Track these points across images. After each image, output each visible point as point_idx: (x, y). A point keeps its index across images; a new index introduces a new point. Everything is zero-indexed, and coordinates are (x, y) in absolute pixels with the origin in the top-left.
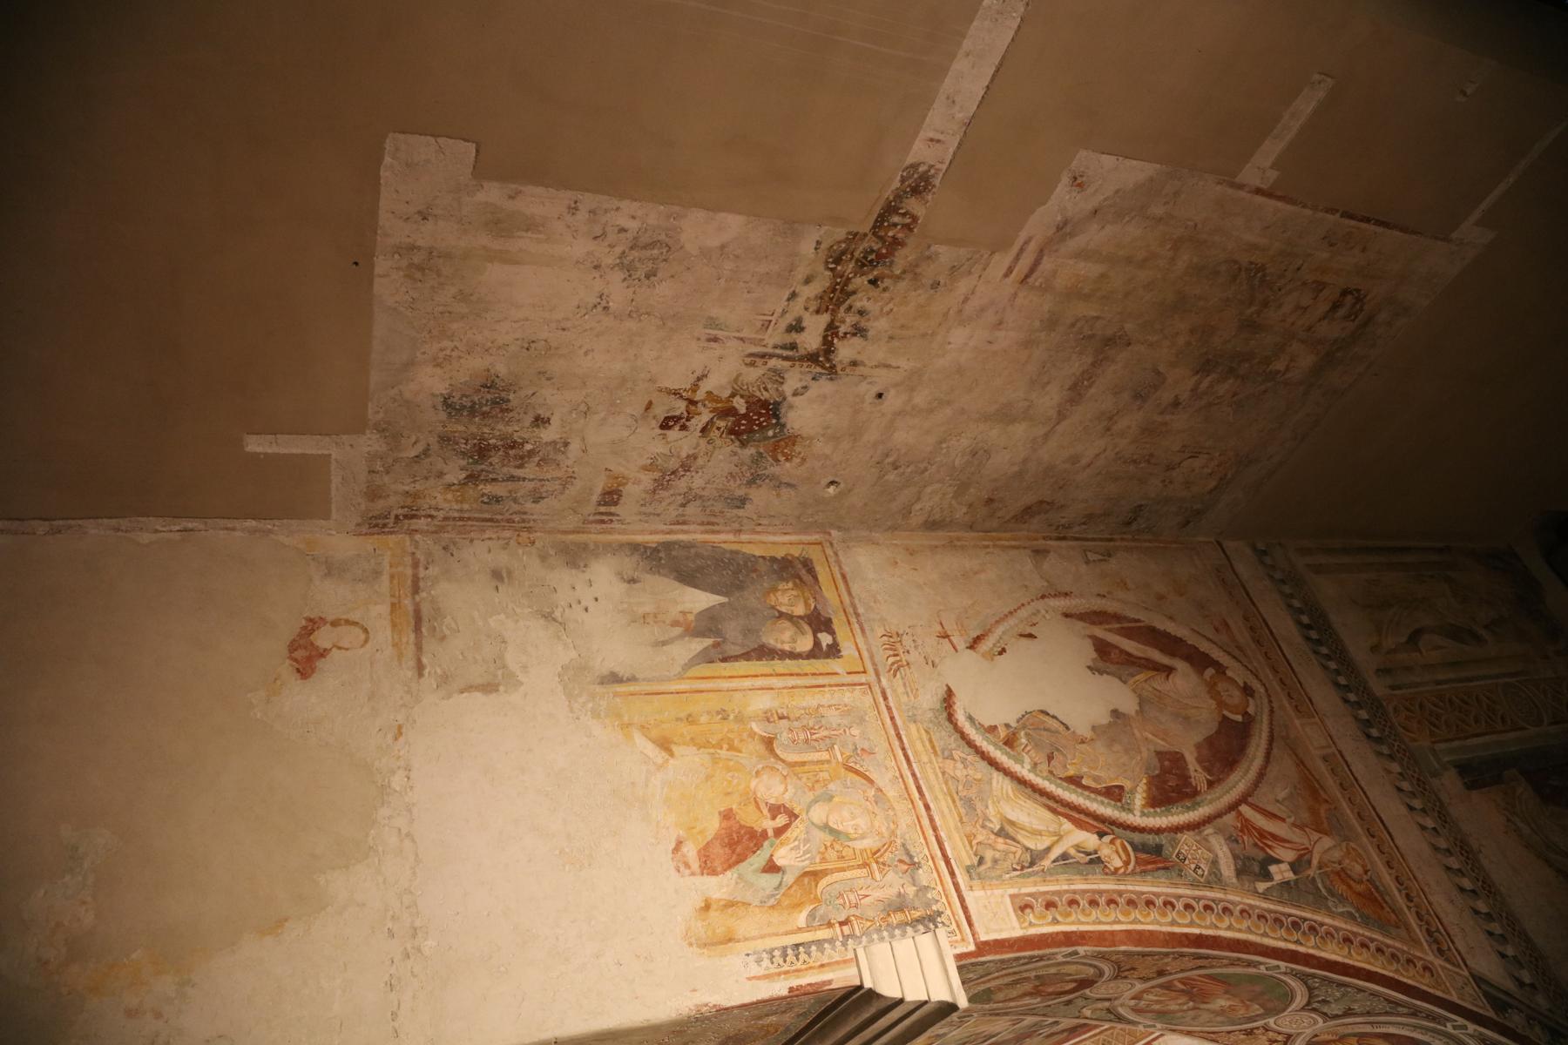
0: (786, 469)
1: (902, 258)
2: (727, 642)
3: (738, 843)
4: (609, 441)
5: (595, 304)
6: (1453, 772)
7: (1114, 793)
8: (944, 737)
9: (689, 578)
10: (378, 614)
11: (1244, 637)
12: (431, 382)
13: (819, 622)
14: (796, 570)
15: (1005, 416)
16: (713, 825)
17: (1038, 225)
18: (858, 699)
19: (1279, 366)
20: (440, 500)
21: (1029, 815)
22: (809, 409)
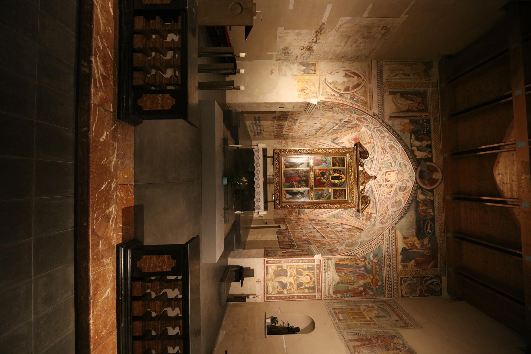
0: (313, 53)
1: (323, 31)
2: (306, 72)
3: (303, 90)
4: (296, 51)
5: (295, 40)
6: (388, 93)
7: (340, 90)
8: (324, 83)
9: (303, 65)
10: (277, 69)
11: (367, 73)
12: (281, 47)
13: (315, 70)
14: (314, 65)
15: (338, 46)
16: (301, 88)
17: (338, 26)
18: (317, 78)
19: (375, 37)
20: (282, 58)
21: (330, 91)
22: (315, 47)
